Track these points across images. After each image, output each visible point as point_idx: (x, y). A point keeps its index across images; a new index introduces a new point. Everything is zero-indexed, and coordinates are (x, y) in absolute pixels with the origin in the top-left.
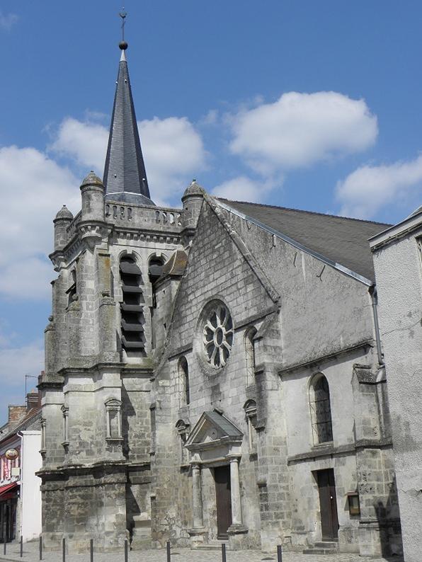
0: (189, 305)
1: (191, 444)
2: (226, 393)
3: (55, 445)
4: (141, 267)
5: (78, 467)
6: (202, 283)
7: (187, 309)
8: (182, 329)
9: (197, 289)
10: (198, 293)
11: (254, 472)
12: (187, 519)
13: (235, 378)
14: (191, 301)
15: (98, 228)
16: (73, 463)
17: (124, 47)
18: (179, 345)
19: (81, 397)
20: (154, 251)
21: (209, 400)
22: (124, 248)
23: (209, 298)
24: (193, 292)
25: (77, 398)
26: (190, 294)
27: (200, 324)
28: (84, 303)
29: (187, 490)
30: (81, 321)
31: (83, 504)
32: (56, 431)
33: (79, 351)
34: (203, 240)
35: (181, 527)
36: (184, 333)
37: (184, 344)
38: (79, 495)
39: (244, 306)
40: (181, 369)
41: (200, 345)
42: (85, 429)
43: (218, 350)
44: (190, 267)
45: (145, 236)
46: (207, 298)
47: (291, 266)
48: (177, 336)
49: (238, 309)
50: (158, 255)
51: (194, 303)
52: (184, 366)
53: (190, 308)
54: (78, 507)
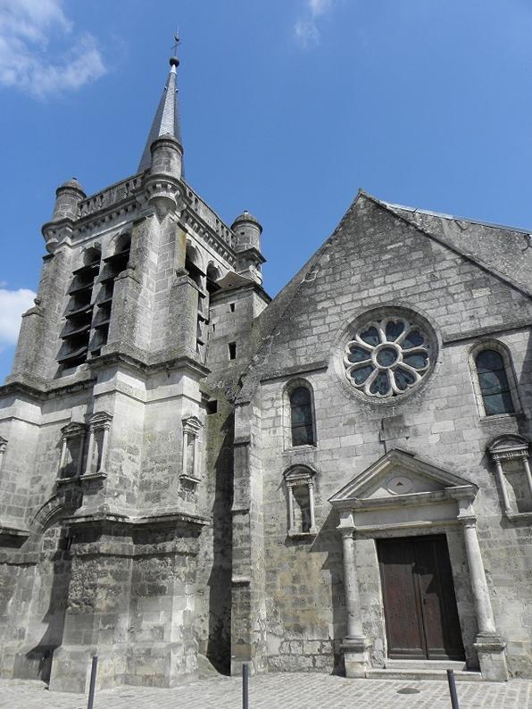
0: (323, 314)
1: (344, 498)
2: (420, 428)
3: (14, 485)
5: (120, 520)
6: (354, 288)
8: (299, 343)
9: (341, 294)
10: (349, 298)
11: (517, 546)
12: (302, 622)
13: (448, 407)
16: (111, 511)
17: (173, 62)
18: (290, 364)
19: (130, 406)
20: (213, 259)
21: (375, 438)
25: (125, 405)
26: (322, 301)
27: (344, 338)
29: (303, 573)
30: (139, 299)
31: (114, 588)
32: (19, 464)
33: (133, 338)
35: (281, 637)
36: (304, 349)
37: (303, 361)
38: (111, 572)
39: (465, 315)
40: (286, 397)
41: (339, 364)
42: (130, 458)
43: (383, 373)
44: (321, 269)
49: (452, 319)
51: (330, 311)
53: (324, 317)
54: (107, 595)
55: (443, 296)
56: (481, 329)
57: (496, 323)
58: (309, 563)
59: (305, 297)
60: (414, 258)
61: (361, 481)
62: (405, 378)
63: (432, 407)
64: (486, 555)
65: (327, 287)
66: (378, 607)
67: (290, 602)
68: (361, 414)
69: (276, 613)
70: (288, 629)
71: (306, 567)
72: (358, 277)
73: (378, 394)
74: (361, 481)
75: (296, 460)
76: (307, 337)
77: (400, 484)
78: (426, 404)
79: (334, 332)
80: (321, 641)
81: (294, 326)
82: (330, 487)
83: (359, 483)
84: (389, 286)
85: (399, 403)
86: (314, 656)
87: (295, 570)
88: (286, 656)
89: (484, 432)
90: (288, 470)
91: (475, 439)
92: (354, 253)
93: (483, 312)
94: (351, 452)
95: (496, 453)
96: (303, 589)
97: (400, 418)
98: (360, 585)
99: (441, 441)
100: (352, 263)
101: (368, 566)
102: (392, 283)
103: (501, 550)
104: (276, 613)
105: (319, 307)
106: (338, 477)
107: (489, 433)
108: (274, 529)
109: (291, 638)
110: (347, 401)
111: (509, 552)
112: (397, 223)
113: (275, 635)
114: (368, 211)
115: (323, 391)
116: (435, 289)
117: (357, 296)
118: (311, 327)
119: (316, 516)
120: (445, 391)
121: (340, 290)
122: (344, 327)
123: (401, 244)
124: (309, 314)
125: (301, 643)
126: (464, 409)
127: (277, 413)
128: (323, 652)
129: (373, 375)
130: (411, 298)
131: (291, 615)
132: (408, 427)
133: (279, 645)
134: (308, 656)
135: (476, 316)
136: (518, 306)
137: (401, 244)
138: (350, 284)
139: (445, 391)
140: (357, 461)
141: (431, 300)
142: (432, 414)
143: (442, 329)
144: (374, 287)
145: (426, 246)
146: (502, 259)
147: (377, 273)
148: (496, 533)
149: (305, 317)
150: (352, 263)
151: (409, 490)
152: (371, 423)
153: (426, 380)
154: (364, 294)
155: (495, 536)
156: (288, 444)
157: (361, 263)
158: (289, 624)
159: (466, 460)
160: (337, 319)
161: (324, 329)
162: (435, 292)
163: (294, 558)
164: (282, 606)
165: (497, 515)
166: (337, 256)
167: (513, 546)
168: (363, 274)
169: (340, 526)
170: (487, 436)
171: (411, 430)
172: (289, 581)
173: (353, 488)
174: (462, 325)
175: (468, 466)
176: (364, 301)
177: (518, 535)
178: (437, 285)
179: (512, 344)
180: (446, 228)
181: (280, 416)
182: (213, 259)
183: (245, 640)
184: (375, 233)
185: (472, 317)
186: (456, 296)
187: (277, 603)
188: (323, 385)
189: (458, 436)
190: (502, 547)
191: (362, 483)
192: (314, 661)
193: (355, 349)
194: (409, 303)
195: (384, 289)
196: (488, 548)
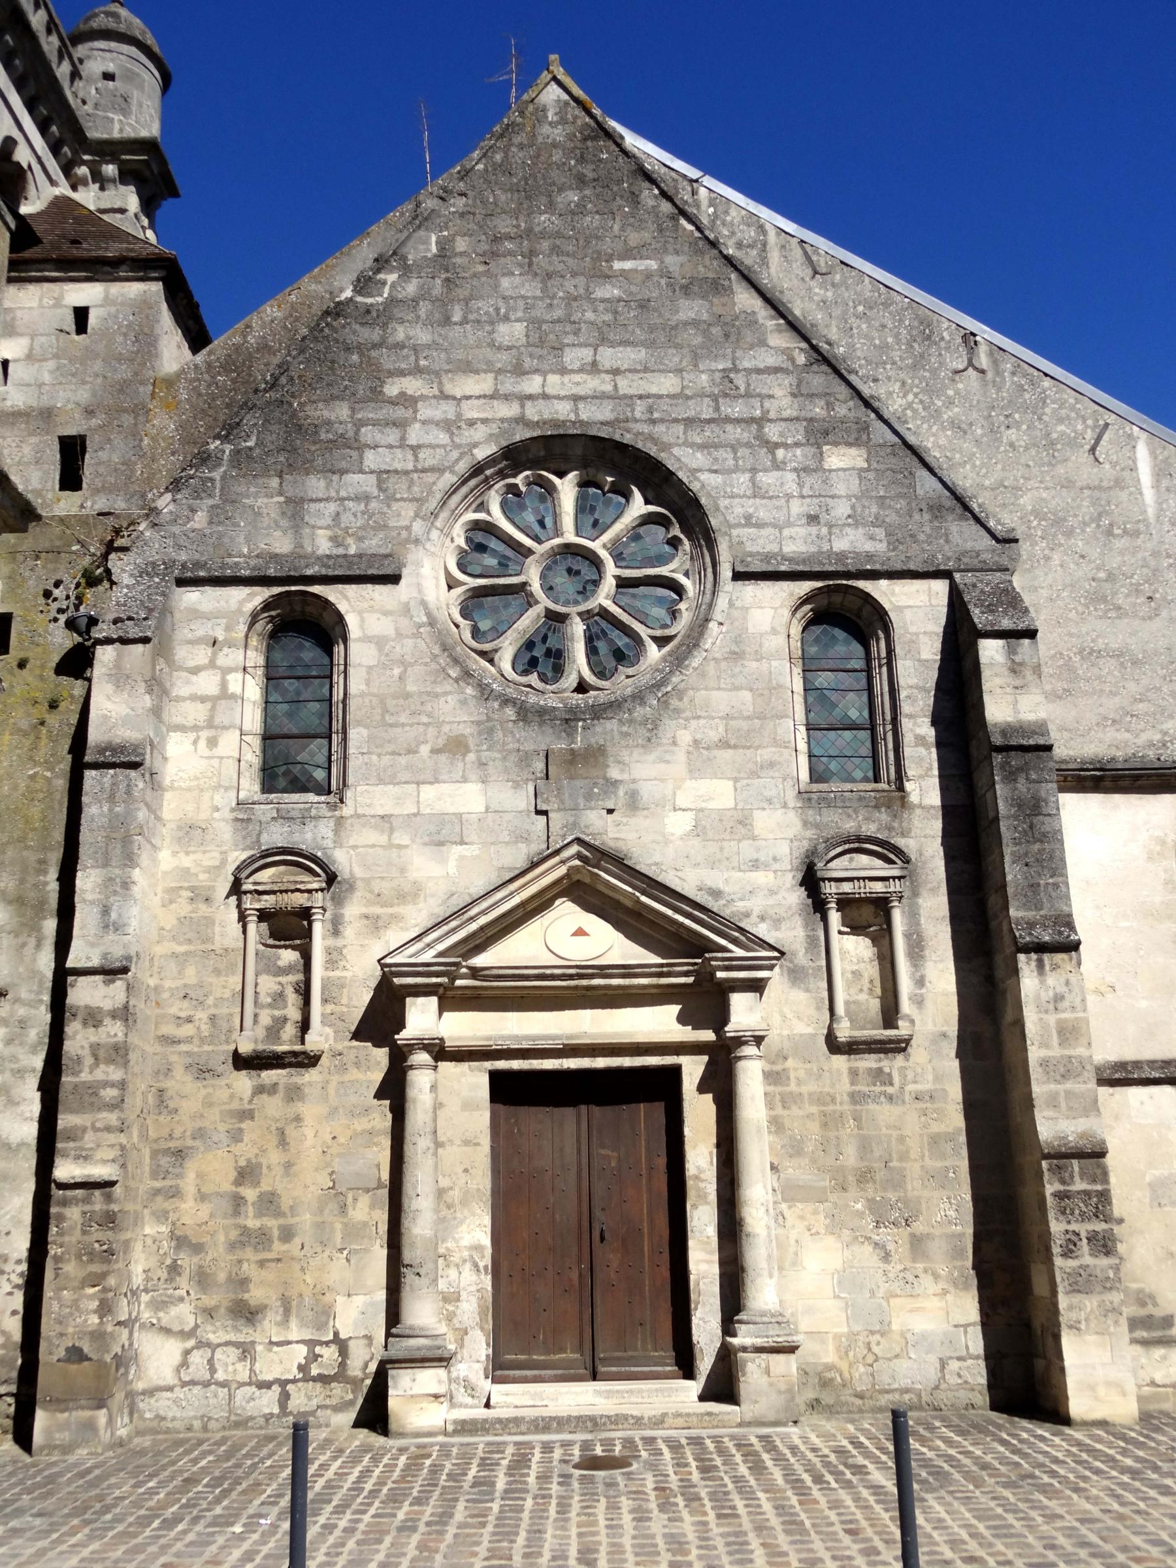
0: (400, 413)
1: (428, 957)
2: (647, 791)
7: (375, 423)
8: (316, 485)
9: (467, 368)
11: (847, 1107)
12: (255, 1295)
13: (724, 744)
14: (407, 401)
18: (282, 544)
20: (16, 134)
21: (522, 800)
23: (555, 423)
24: (418, 371)
26: (402, 373)
27: (456, 498)
35: (184, 1335)
36: (332, 507)
37: (324, 546)
39: (797, 508)
40: (254, 641)
41: (433, 574)
43: (555, 619)
44: (406, 271)
47: (1084, 457)
49: (763, 510)
50: (22, 155)
51: (426, 411)
52: (302, 627)
53: (401, 425)
55: (748, 445)
56: (830, 553)
57: (869, 547)
58: (291, 1132)
59: (348, 349)
60: (682, 316)
61: (483, 912)
62: (614, 645)
63: (685, 737)
64: (776, 1124)
65: (423, 336)
66: (478, 1248)
67: (221, 1238)
68: (486, 730)
69: (174, 1269)
70: (209, 1313)
71: (283, 1142)
73: (533, 679)
74: (483, 912)
75: (276, 836)
76: (343, 472)
77: (580, 932)
78: (669, 727)
79: (429, 478)
80: (311, 1344)
82: (375, 925)
83: (472, 919)
84: (608, 377)
85: (598, 712)
86: (283, 1383)
87: (246, 1151)
88: (197, 1390)
89: (805, 824)
90: (252, 860)
91: (782, 833)
92: (511, 253)
93: (842, 509)
94: (443, 833)
95: (830, 880)
96: (269, 1203)
97: (594, 756)
98: (440, 1193)
99: (698, 830)
100: (505, 282)
101: (467, 1143)
102: (616, 372)
103: (809, 1116)
104: (174, 1269)
105: (392, 389)
106: (403, 897)
107: (817, 826)
108: (187, 1030)
109: (213, 1338)
110: (448, 686)
111: (828, 1121)
112: (649, 195)
113: (167, 1331)
114: (571, 137)
115: (380, 642)
116: (728, 420)
117: (509, 385)
118: (361, 448)
119: (325, 1001)
120: (721, 700)
121: (459, 354)
122: (463, 467)
123: (653, 265)
124: (356, 402)
125: (246, 1351)
126: (766, 754)
127: (224, 685)
128: (314, 1372)
129: (528, 621)
130: (660, 429)
131: (222, 1276)
132: (615, 783)
133: (177, 1358)
134: (265, 1385)
135: (824, 517)
136: (927, 516)
137: (653, 265)
138: (492, 345)
139: (721, 700)
140: (462, 858)
141: (716, 446)
142: (680, 756)
143: (735, 532)
144: (563, 371)
145: (716, 287)
146: (904, 383)
147: (576, 333)
148: (801, 1074)
149: (342, 411)
150: (505, 282)
151: (606, 944)
152: (513, 758)
153: (678, 661)
154: (533, 384)
155: (799, 1082)
156: (251, 787)
157: (531, 288)
158: (209, 1301)
159: (758, 890)
160: (443, 438)
161: (401, 460)
162: (729, 428)
163: (247, 1115)
164: (198, 1248)
165: (810, 1030)
166: (461, 244)
167: (838, 1107)
168: (535, 323)
169: (404, 1034)
170: (809, 833)
171: (621, 793)
172: (224, 1180)
173: (453, 931)
174: (786, 532)
175: (756, 904)
176: (529, 404)
177: (852, 1084)
178: (736, 409)
179: (900, 609)
180: (774, 257)
181: (233, 697)
182: (16, 134)
183: (86, 1349)
184: (580, 210)
185: (813, 519)
186: (780, 453)
187: (181, 1241)
188: (380, 626)
189: (742, 822)
190: (814, 1109)
191: (483, 920)
192: (285, 1397)
193: (482, 535)
194: (651, 438)
195: (602, 384)
196: (779, 1111)
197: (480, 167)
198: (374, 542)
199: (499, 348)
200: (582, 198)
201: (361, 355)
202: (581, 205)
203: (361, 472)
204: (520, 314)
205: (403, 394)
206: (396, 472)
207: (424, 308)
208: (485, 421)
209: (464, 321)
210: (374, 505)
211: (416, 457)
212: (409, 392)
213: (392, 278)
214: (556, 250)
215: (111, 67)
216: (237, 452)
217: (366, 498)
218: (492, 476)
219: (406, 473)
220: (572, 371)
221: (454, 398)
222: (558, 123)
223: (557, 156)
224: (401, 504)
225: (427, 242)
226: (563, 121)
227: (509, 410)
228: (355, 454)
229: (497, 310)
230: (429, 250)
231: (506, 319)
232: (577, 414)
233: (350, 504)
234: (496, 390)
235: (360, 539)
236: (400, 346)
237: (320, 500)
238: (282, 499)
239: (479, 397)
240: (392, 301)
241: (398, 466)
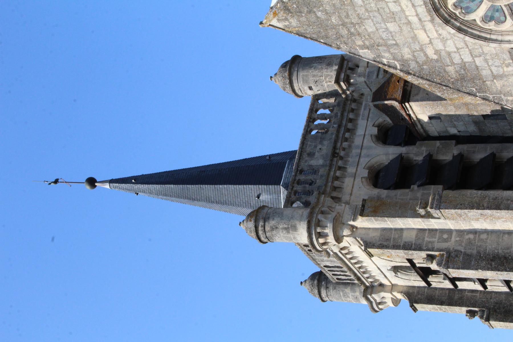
0: (443, 53)
4: (391, 157)
6: (404, 28)
8: (485, 73)
9: (415, 38)
10: (422, 36)
14: (437, 52)
15: (320, 217)
20: (368, 137)
22: (358, 180)
23: (429, 11)
24: (422, 50)
26: (426, 55)
28: (437, 245)
30: (469, 252)
34: (334, 27)
36: (494, 69)
45: (344, 149)
46: (429, 18)
48: (498, 84)
50: (375, 131)
51: (440, 46)
53: (449, 54)
59: (423, 69)
72: (388, 25)
79: (470, 44)
81: (463, 78)
92: (356, 29)
100: (370, 30)
105: (435, 57)
114: (292, 17)
121: (410, 40)
122: (461, 36)
144: (403, 11)
147: (384, 9)
149: (451, 69)
154: (414, 19)
166: (360, 43)
168: (384, 21)
176: (423, 20)
197: (322, 41)
198: (505, 56)
199: (401, 30)
200: (319, 11)
201: (423, 65)
202: (322, 11)
203: (475, 61)
204: (383, 25)
205: (435, 54)
206: (471, 53)
207: (392, 50)
208: (437, 31)
209: (394, 40)
210: (488, 57)
211: (461, 48)
212: (433, 52)
213: (385, 61)
214: (347, 16)
215: (306, 88)
216: (479, 92)
217: (486, 61)
218: (459, 22)
219: (470, 50)
220: (401, 8)
221: (430, 40)
222: (288, 21)
223: (303, 19)
224: (484, 50)
225: (365, 53)
226: (286, 19)
227: (429, 26)
228: (467, 65)
229: (384, 32)
230: (367, 52)
231: (387, 29)
232: (421, 5)
233: (490, 64)
234: (421, 29)
235: (505, 60)
236: (414, 56)
237: (491, 71)
238: (495, 81)
239: (427, 34)
240: (394, 59)
241: (468, 53)
